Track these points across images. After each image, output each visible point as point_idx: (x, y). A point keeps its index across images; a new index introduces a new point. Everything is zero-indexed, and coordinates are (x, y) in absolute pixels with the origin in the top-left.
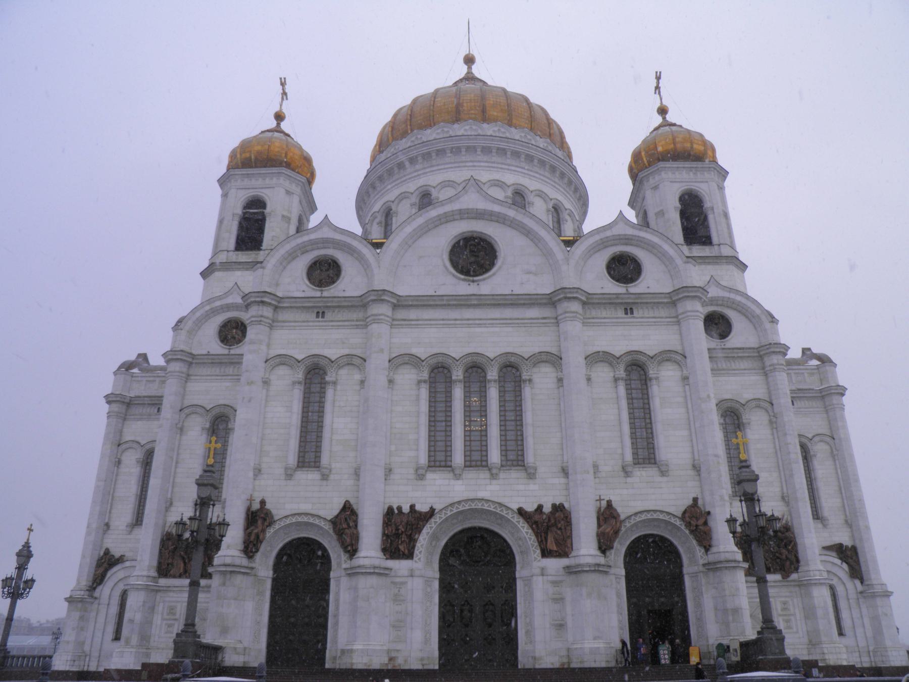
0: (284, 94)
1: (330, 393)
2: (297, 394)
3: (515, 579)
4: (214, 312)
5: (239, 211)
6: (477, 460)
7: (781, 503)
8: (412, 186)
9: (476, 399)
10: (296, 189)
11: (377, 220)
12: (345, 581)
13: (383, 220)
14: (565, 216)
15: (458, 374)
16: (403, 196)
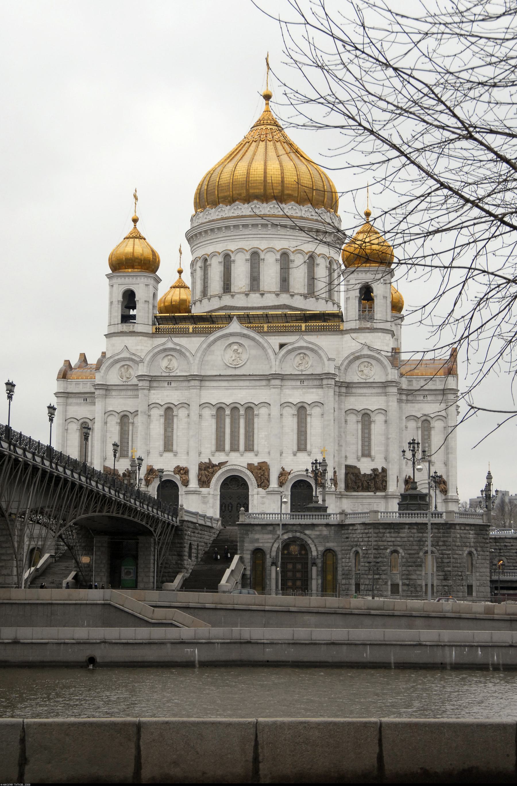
0: (136, 199)
1: (175, 420)
2: (162, 420)
3: (248, 495)
4: (117, 361)
5: (121, 299)
6: (234, 448)
7: (384, 460)
8: (220, 247)
9: (235, 422)
10: (151, 282)
11: (200, 264)
12: (184, 496)
13: (203, 265)
14: (319, 260)
15: (228, 412)
16: (214, 254)
